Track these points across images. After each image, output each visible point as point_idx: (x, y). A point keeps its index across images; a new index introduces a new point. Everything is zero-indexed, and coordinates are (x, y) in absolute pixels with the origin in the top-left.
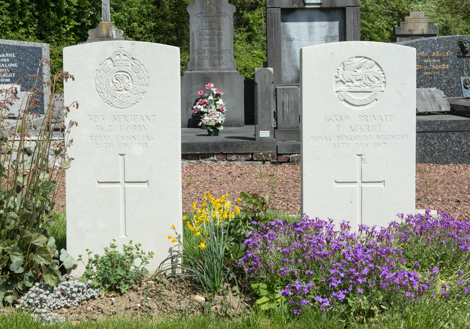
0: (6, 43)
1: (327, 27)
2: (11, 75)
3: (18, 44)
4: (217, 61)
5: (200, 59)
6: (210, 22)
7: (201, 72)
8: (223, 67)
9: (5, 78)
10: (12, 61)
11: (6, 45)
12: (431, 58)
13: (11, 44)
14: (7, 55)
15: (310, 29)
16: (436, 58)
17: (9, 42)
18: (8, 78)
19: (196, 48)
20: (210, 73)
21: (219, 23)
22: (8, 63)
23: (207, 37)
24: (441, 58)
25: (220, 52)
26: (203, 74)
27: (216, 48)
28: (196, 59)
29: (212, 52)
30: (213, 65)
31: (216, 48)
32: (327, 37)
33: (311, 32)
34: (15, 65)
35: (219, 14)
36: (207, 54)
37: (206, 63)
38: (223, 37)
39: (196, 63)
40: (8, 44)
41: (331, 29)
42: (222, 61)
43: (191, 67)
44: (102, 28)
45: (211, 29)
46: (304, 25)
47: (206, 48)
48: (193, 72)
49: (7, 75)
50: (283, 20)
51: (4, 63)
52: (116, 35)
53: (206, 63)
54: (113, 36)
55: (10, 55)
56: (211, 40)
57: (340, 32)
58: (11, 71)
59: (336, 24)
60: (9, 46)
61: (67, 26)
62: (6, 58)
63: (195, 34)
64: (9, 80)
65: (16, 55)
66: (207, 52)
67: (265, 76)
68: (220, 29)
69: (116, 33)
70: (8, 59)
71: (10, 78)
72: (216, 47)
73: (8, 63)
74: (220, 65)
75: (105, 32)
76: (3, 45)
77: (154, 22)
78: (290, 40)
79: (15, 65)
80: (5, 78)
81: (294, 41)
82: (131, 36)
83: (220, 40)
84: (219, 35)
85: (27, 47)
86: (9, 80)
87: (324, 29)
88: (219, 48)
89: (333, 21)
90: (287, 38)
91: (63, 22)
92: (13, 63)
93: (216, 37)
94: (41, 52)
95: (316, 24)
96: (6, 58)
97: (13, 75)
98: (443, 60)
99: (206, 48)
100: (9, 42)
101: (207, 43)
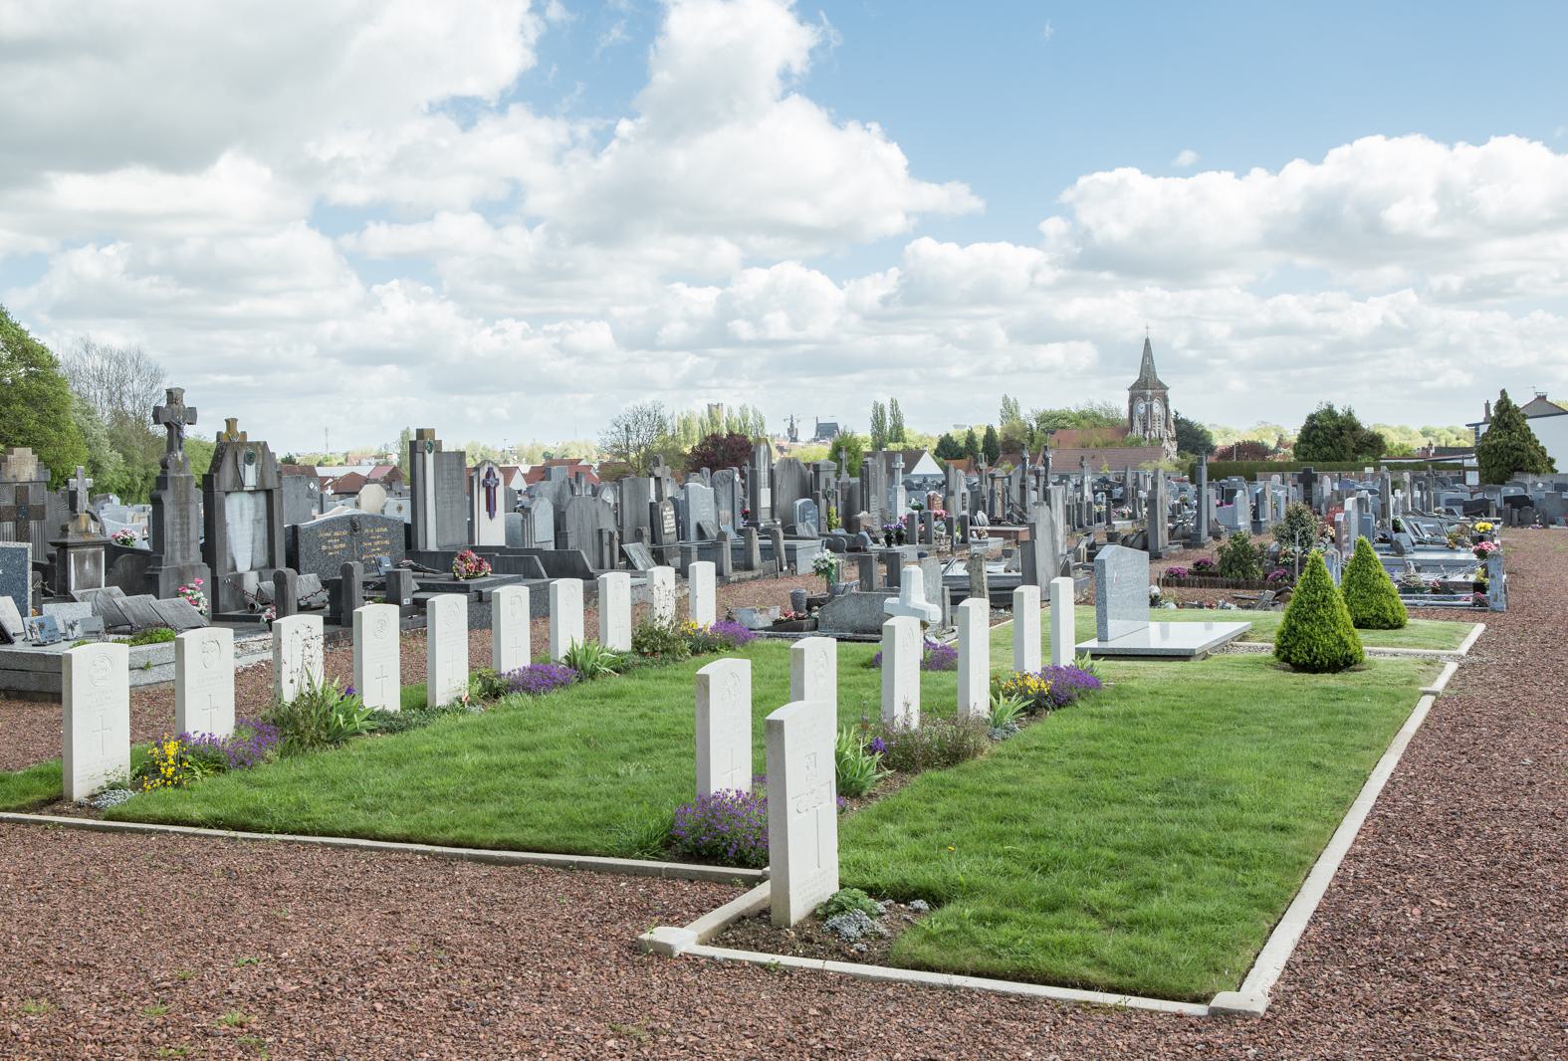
6: (181, 510)
8: (192, 559)
16: (337, 538)
25: (188, 544)
27: (185, 539)
29: (182, 543)
30: (183, 558)
31: (185, 539)
35: (187, 502)
36: (178, 546)
37: (178, 559)
45: (181, 517)
56: (182, 529)
83: (188, 529)
84: (188, 524)
101: (178, 533)
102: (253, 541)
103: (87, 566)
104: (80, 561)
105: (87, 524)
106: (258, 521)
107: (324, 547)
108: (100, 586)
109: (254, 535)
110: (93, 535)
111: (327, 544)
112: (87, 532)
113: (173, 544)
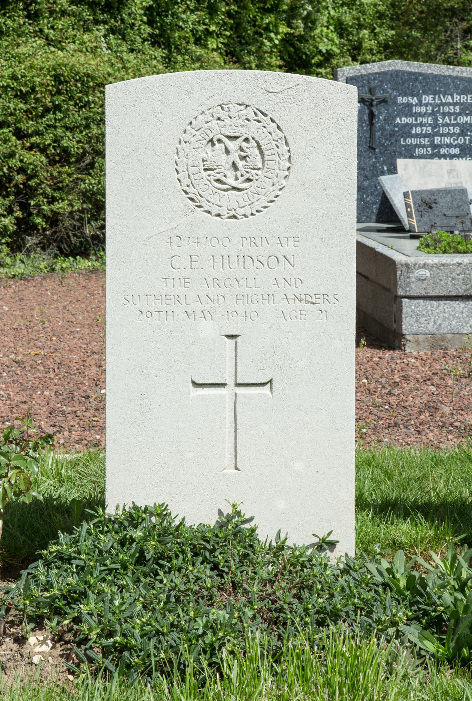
0: (455, 74)
2: (461, 141)
9: (449, 146)
11: (457, 77)
17: (462, 72)
18: (455, 146)
40: (459, 75)
49: (454, 140)
51: (450, 114)
58: (463, 133)
61: (272, 35)
62: (455, 104)
70: (457, 107)
76: (450, 76)
77: (393, 29)
80: (449, 146)
82: (354, 59)
86: (457, 151)
91: (267, 29)
96: (455, 104)
97: (465, 140)
100: (462, 72)
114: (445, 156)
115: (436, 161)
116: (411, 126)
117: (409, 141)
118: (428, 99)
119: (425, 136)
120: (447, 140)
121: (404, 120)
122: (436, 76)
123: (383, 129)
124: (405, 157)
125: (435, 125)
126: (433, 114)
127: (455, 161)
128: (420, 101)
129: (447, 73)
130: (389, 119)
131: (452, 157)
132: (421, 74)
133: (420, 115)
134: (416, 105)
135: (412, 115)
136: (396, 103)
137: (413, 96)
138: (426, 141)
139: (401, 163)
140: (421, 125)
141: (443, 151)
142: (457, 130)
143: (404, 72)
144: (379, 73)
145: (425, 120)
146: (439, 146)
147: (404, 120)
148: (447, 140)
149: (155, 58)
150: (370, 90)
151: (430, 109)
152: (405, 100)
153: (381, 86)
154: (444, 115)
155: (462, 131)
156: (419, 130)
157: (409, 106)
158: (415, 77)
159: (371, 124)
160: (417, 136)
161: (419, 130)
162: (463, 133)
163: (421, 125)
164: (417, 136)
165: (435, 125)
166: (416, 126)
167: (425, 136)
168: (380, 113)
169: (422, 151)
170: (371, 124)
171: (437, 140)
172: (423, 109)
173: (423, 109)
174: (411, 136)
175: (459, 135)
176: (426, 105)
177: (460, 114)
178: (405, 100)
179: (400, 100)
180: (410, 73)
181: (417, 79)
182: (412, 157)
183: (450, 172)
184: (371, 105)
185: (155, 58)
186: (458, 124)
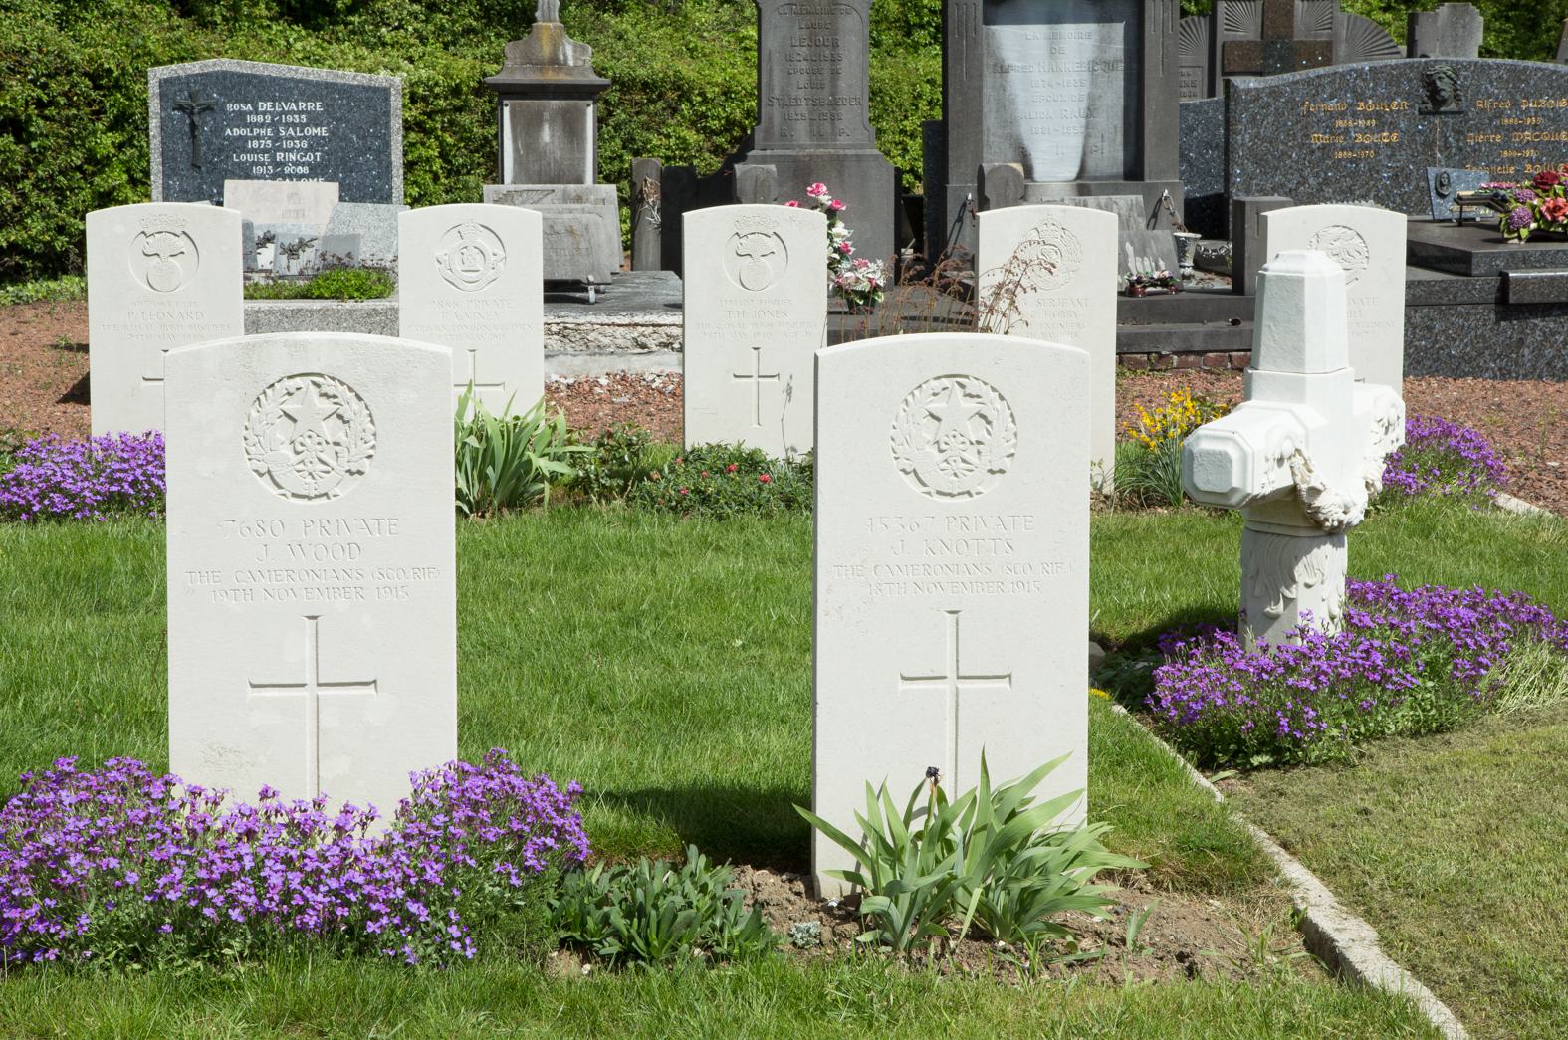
0: (298, 76)
1: (1095, 37)
2: (309, 158)
3: (330, 79)
4: (827, 127)
5: (787, 120)
6: (812, 27)
7: (788, 152)
8: (842, 140)
9: (296, 164)
10: (314, 120)
11: (300, 80)
12: (1355, 116)
13: (311, 77)
14: (302, 105)
15: (1053, 42)
16: (1367, 116)
19: (776, 92)
20: (811, 157)
21: (835, 31)
22: (303, 126)
23: (804, 65)
24: (1378, 116)
25: (834, 104)
26: (795, 160)
27: (826, 95)
28: (777, 120)
29: (815, 103)
30: (818, 136)
31: (826, 95)
32: (1095, 62)
33: (1053, 51)
34: (322, 132)
36: (803, 109)
37: (801, 131)
38: (844, 65)
39: (776, 130)
41: (1104, 41)
42: (841, 125)
43: (765, 139)
44: (539, 39)
45: (814, 43)
46: (1037, 32)
47: (802, 93)
48: (768, 152)
50: (988, 21)
51: (294, 126)
52: (576, 58)
53: (801, 131)
54: (566, 59)
55: (310, 106)
56: (814, 72)
57: (1126, 51)
58: (310, 149)
59: (1119, 29)
60: (307, 82)
62: (300, 113)
63: (775, 56)
64: (305, 170)
65: (325, 106)
66: (804, 103)
67: (1007, 184)
68: (835, 45)
69: (575, 51)
70: (303, 117)
71: (309, 164)
72: (827, 89)
73: (303, 126)
74: (835, 135)
75: (546, 50)
76: (292, 79)
78: (1002, 69)
79: (322, 132)
80: (296, 164)
81: (1012, 73)
83: (835, 73)
85: (352, 86)
86: (305, 170)
87: (1087, 42)
88: (833, 94)
89: (1111, 20)
90: (995, 65)
92: (316, 126)
93: (826, 66)
94: (387, 99)
95: (1069, 29)
96: (300, 113)
98: (1382, 122)
99: (802, 93)
101: (803, 79)
102: (1090, 112)
103: (546, 135)
104: (527, 128)
105: (556, 45)
106: (1109, 65)
107: (1318, 139)
108: (580, 180)
109: (1092, 97)
110: (571, 70)
111: (1332, 131)
112: (555, 62)
113: (786, 102)
114: (290, 177)
115: (278, 183)
116: (245, 139)
117: (243, 157)
118: (265, 106)
119: (265, 151)
120: (292, 157)
121: (237, 132)
122: (273, 79)
123: (209, 143)
124: (240, 178)
125: (276, 139)
126: (274, 125)
127: (303, 183)
128: (256, 108)
129: (288, 75)
130: (218, 131)
131: (299, 177)
132: (255, 76)
133: (256, 125)
134: (250, 113)
135: (246, 126)
136: (223, 110)
137: (246, 103)
138: (266, 158)
139: (229, 184)
140: (258, 138)
141: (287, 170)
142: (305, 145)
143: (233, 74)
144: (201, 75)
145: (263, 132)
146: (283, 164)
147: (237, 132)
148: (292, 157)
149: (42, 16)
150: (190, 95)
151: (268, 119)
152: (236, 107)
153: (204, 90)
154: (287, 125)
155: (310, 146)
156: (255, 144)
157: (242, 115)
158: (249, 79)
159: (194, 137)
160: (253, 151)
161: (255, 144)
162: (310, 149)
163: (258, 138)
164: (253, 151)
165: (276, 139)
166: (252, 139)
167: (265, 151)
168: (206, 124)
169: (260, 170)
170: (194, 137)
171: (280, 156)
172: (260, 119)
173: (260, 119)
174: (246, 151)
175: (306, 151)
176: (264, 114)
177: (307, 125)
178: (236, 107)
179: (229, 107)
180: (241, 75)
181: (249, 82)
182: (248, 176)
183: (290, 196)
184: (191, 114)
185: (42, 16)
186: (305, 138)
